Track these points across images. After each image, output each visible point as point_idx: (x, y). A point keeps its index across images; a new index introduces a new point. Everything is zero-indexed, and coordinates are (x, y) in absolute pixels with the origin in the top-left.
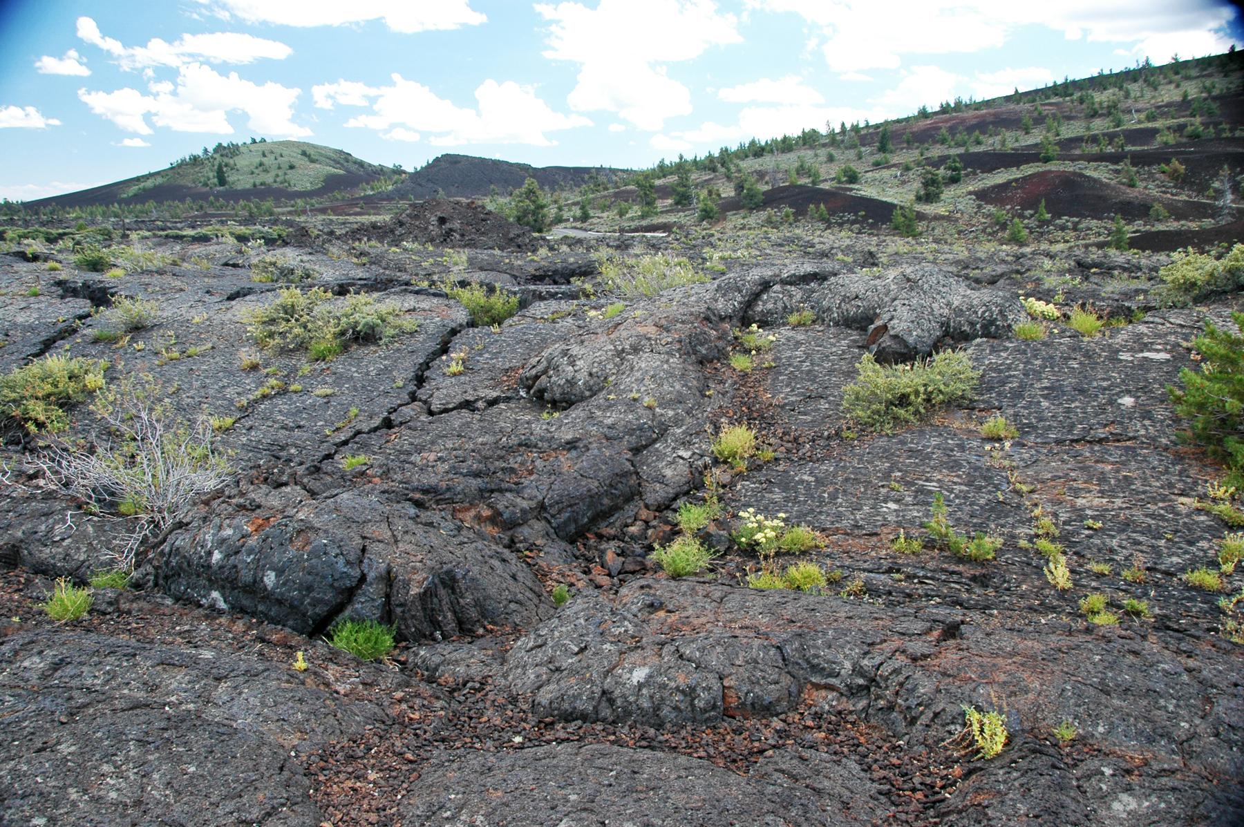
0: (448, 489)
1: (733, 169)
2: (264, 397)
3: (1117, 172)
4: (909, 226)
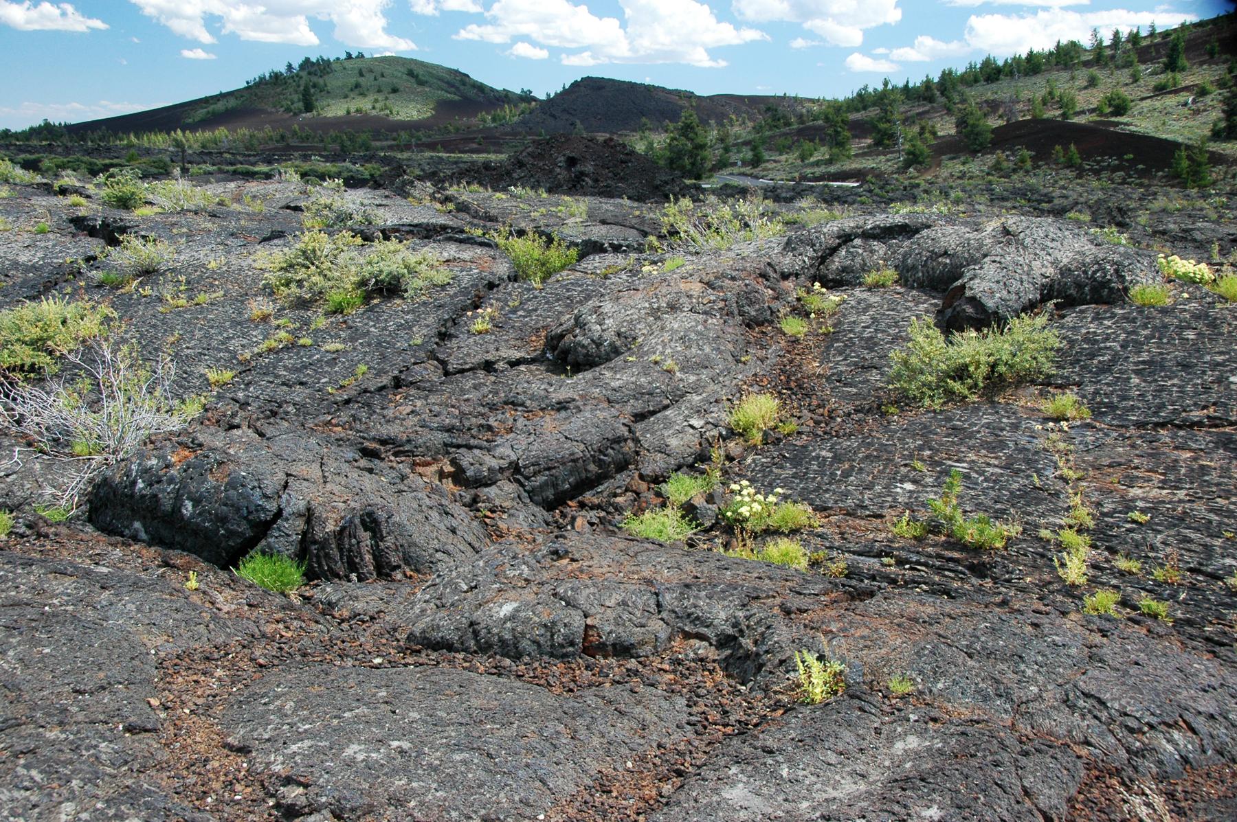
0: (409, 441)
1: (957, 99)
2: (270, 350)
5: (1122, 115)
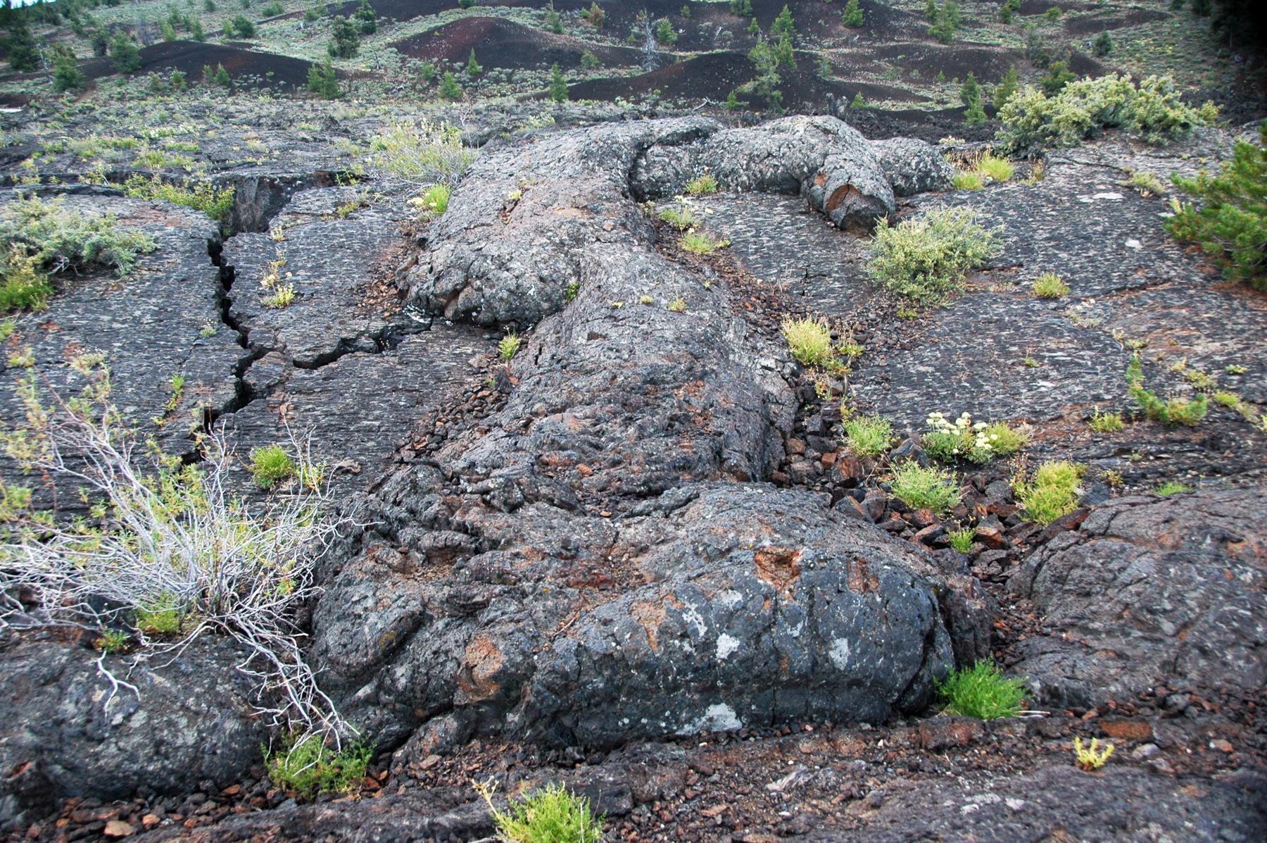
1: (83, 21)
3: (541, 17)
4: (329, 87)
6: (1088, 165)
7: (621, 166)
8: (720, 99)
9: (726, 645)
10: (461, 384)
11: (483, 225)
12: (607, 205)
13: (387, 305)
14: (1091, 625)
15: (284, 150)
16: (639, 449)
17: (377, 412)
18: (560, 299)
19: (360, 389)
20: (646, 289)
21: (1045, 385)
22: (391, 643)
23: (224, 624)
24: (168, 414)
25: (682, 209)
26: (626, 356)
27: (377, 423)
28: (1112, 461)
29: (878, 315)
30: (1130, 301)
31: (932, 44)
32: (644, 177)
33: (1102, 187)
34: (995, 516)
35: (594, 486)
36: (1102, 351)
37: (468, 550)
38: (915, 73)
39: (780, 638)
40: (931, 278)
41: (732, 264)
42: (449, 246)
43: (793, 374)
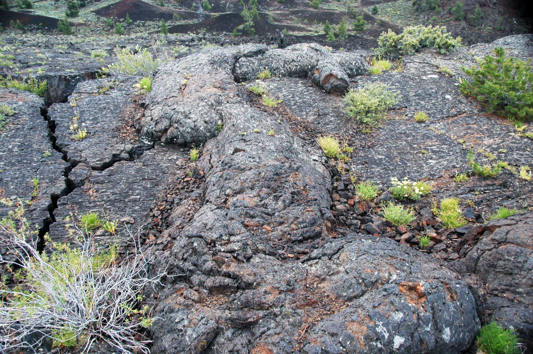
4: (67, 30)
5: (30, 8)
6: (420, 63)
7: (229, 67)
8: (230, 32)
9: (398, 341)
10: (175, 174)
11: (173, 97)
12: (229, 86)
13: (132, 136)
14: (517, 290)
15: (53, 58)
16: (290, 215)
17: (137, 191)
18: (215, 131)
19: (127, 180)
20: (255, 125)
21: (432, 162)
22: (204, 347)
23: (100, 335)
24: (33, 198)
25: (259, 86)
26: (258, 160)
27: (138, 197)
28: (467, 195)
29: (354, 132)
30: (453, 122)
31: (312, 9)
32: (239, 71)
33: (429, 72)
34: (430, 226)
35: (276, 238)
36: (450, 145)
37: (233, 287)
38: (306, 21)
39: (422, 334)
40: (374, 115)
41: (285, 110)
42: (159, 107)
43: (326, 162)
